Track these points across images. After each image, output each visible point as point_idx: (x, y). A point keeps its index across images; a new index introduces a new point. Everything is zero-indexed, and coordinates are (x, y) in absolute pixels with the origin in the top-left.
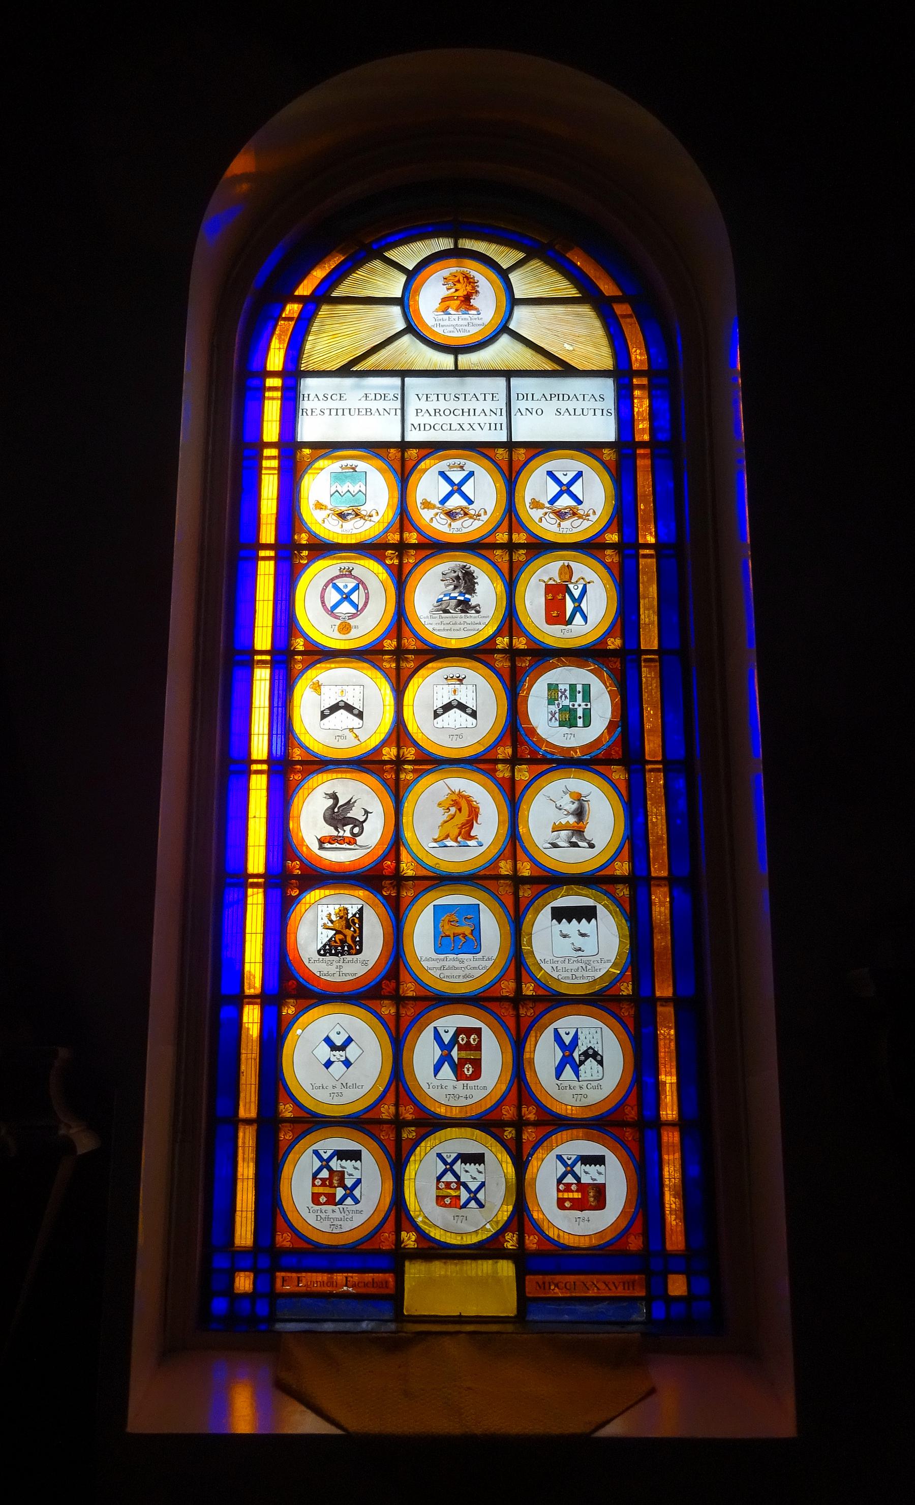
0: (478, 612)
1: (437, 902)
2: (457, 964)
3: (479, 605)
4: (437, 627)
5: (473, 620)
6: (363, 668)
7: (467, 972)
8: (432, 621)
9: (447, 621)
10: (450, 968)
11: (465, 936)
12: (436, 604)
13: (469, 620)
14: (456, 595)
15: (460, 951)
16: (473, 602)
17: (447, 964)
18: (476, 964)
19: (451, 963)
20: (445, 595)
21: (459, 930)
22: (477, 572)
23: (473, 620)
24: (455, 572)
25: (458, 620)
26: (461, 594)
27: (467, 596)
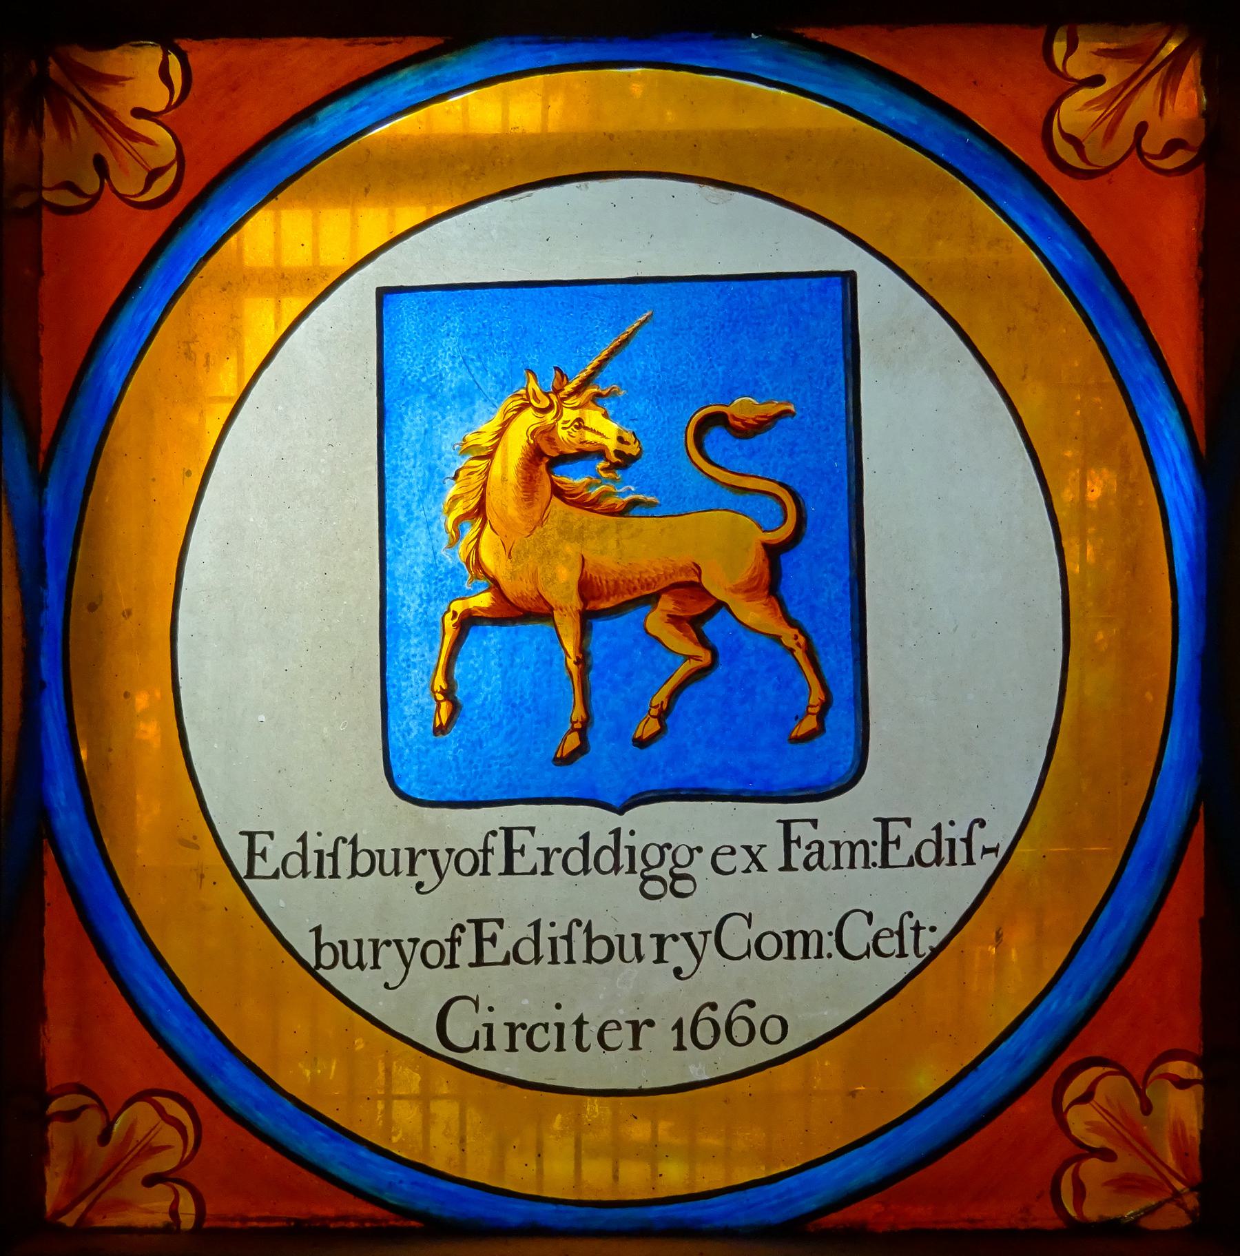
1: (410, 265)
2: (614, 902)
7: (721, 982)
10: (542, 946)
11: (695, 605)
15: (660, 764)
17: (516, 901)
18: (812, 900)
19: (556, 899)
21: (637, 549)
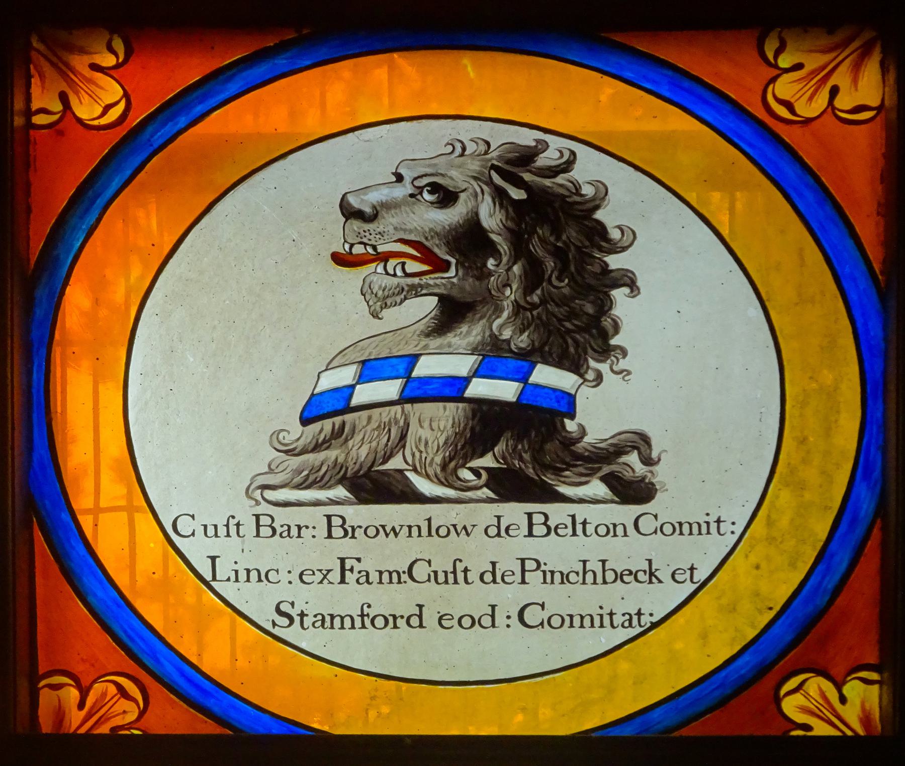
0: (633, 492)
3: (640, 442)
4: (314, 599)
5: (591, 548)
6: (234, 75)
8: (269, 553)
9: (396, 553)
12: (295, 432)
13: (560, 552)
14: (462, 365)
16: (598, 414)
20: (370, 370)
22: (626, 201)
23: (591, 548)
24: (446, 197)
25: (477, 552)
26: (493, 357)
27: (545, 375)
